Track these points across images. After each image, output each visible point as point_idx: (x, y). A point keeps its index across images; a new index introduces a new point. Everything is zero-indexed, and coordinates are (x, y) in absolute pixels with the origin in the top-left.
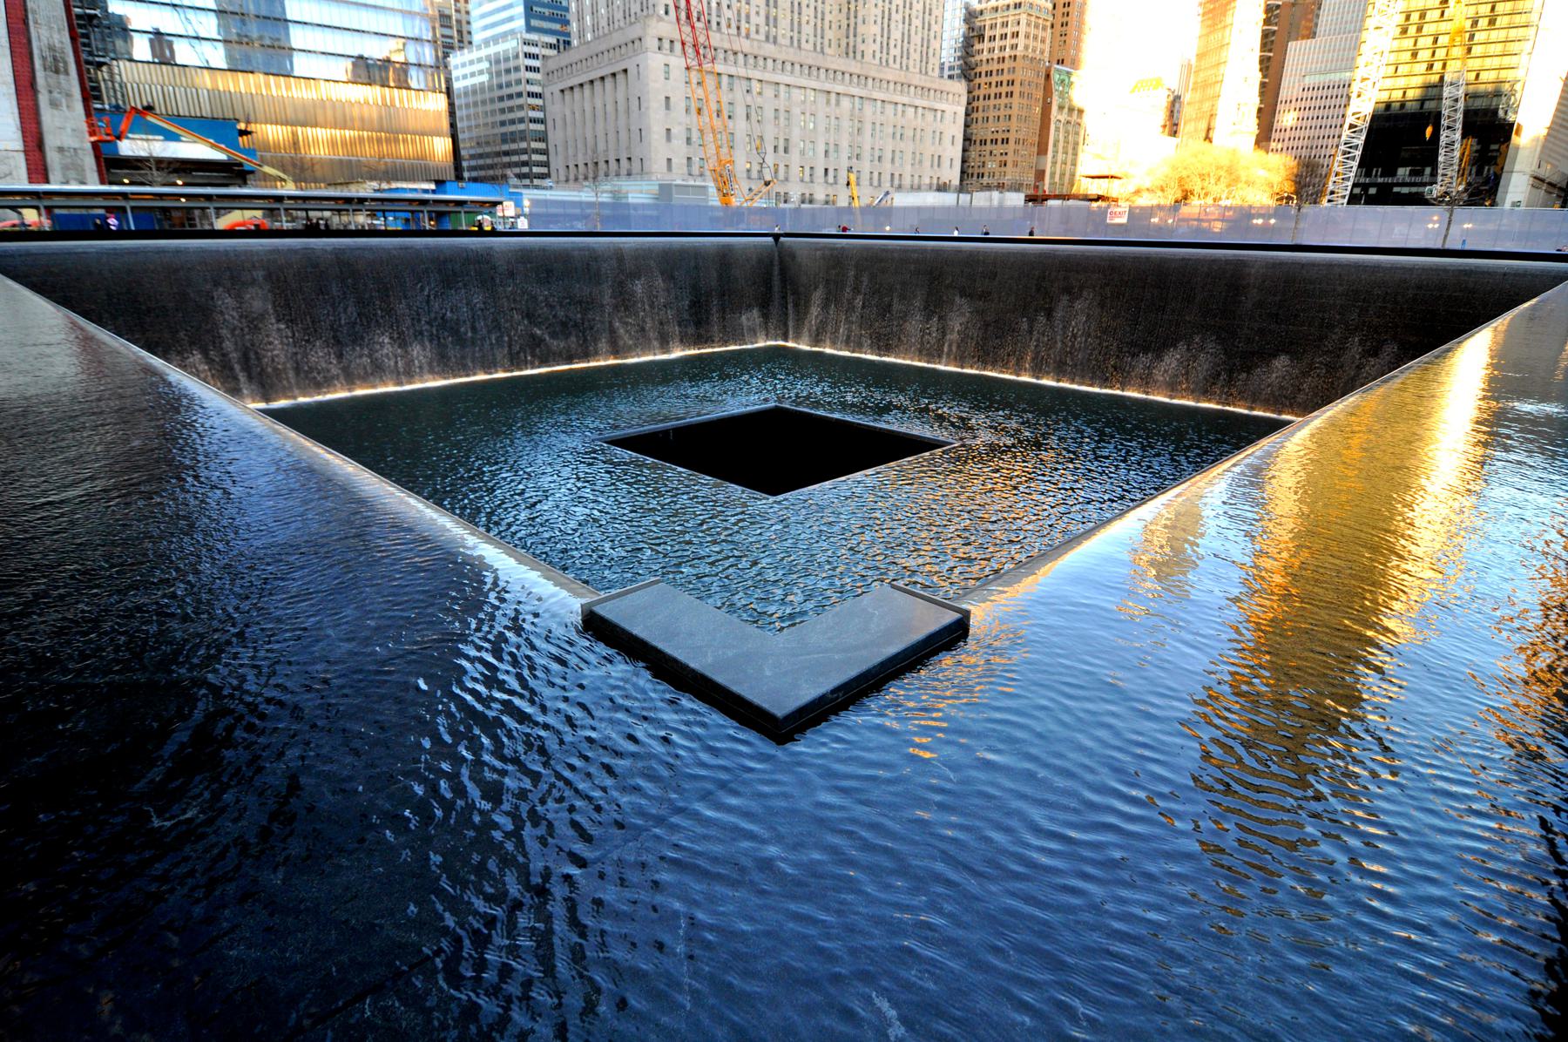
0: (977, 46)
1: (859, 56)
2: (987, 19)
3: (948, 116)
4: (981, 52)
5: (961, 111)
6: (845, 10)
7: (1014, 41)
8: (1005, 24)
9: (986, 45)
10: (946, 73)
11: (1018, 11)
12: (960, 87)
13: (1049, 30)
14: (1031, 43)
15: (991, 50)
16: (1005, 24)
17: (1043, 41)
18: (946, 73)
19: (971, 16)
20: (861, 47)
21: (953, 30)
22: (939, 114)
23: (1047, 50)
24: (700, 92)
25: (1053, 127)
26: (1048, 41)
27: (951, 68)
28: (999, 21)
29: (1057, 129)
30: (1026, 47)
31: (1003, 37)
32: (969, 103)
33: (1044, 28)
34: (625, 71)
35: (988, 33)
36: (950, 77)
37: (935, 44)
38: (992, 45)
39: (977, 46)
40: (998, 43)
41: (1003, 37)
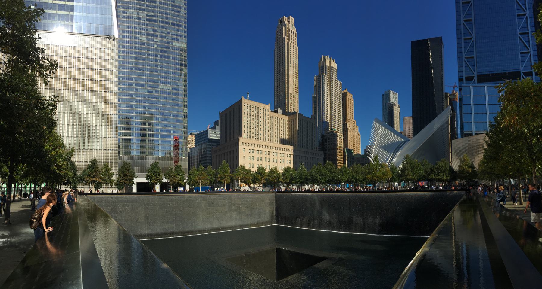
0: (325, 144)
5: (323, 158)
8: (332, 139)
9: (327, 143)
10: (318, 149)
11: (334, 136)
12: (322, 153)
13: (343, 140)
15: (329, 144)
16: (332, 139)
17: (342, 142)
18: (318, 149)
19: (323, 137)
21: (319, 139)
22: (317, 159)
23: (343, 144)
24: (253, 155)
26: (343, 142)
27: (319, 148)
28: (330, 138)
31: (332, 141)
32: (324, 156)
33: (342, 140)
34: (233, 150)
35: (328, 140)
36: (319, 150)
37: (314, 143)
38: (329, 143)
40: (330, 143)
41: (332, 141)
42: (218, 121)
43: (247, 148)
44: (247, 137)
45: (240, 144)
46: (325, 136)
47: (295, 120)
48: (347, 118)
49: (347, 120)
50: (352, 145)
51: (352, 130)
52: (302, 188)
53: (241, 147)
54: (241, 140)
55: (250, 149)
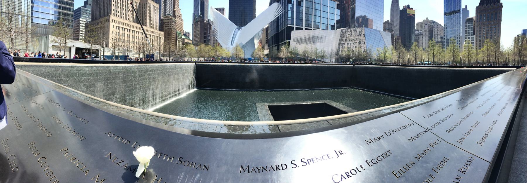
1: (145, 25)
2: (165, 21)
3: (161, 38)
4: (164, 27)
6: (142, 17)
7: (170, 25)
9: (165, 26)
11: (171, 20)
12: (162, 33)
14: (174, 26)
20: (145, 24)
25: (178, 41)
29: (178, 42)
30: (173, 27)
35: (165, 24)
39: (164, 26)
42: (223, 15)
43: (115, 25)
44: (120, 17)
45: (111, 20)
46: (164, 20)
47: (145, 4)
48: (175, 6)
49: (175, 8)
50: (178, 29)
51: (178, 17)
52: (201, 59)
53: (111, 24)
54: (112, 17)
55: (117, 26)
